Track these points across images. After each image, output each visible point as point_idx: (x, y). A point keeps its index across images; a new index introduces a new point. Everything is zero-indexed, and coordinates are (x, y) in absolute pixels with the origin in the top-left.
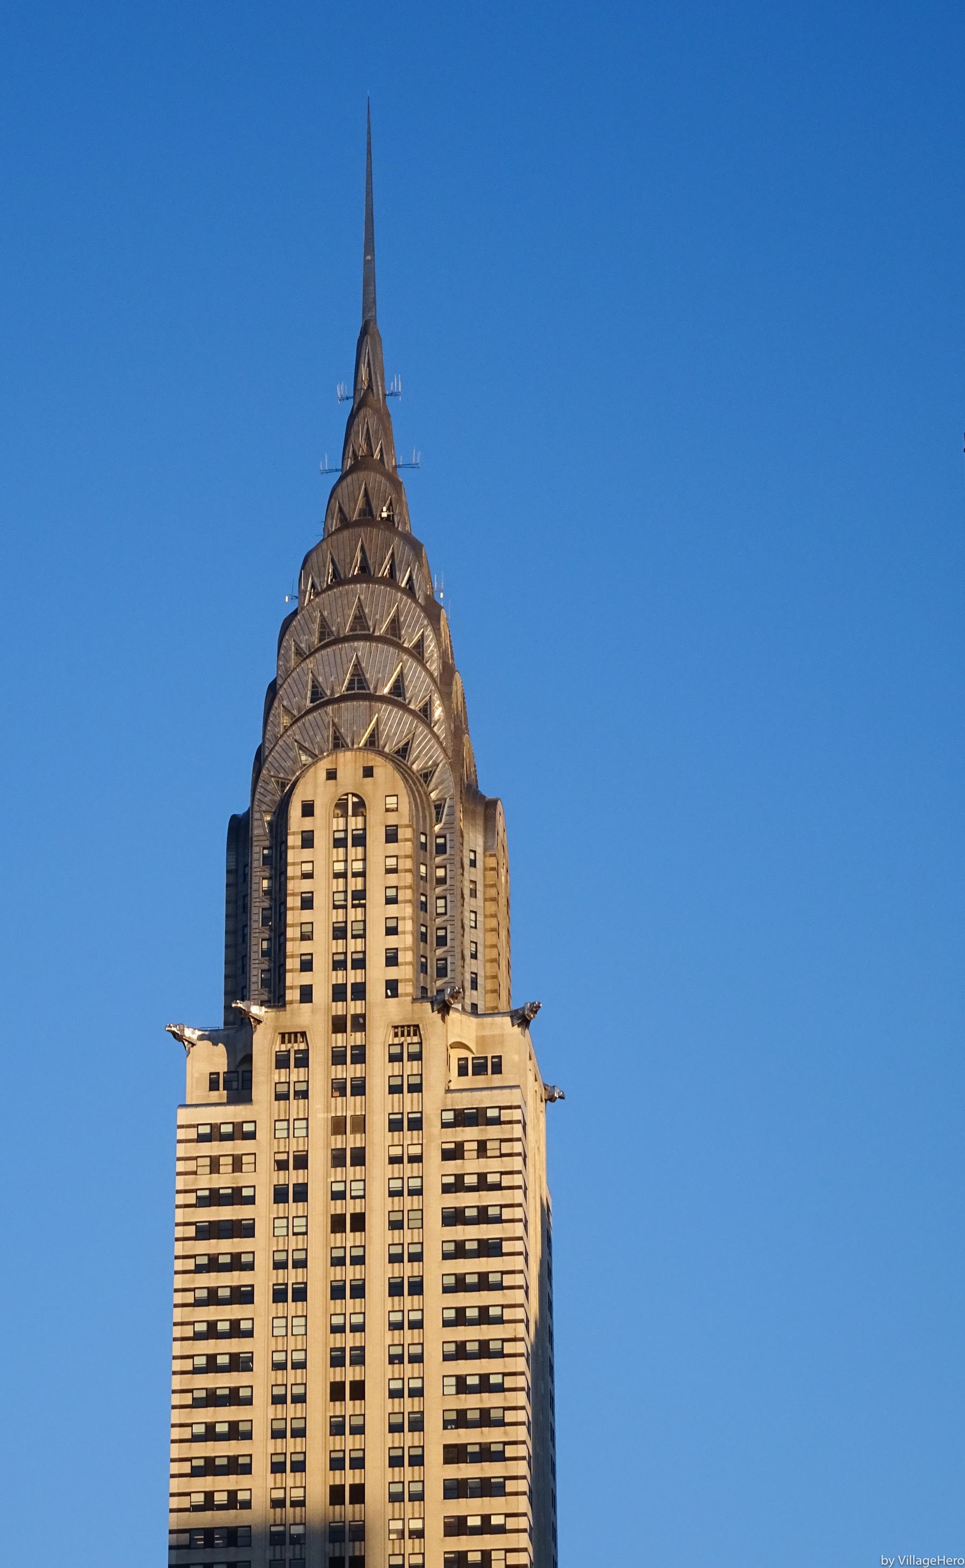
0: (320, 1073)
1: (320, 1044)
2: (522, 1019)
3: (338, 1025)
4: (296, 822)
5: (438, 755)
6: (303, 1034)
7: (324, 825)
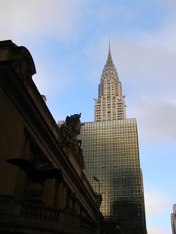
3: (108, 97)
5: (116, 77)
7: (106, 83)
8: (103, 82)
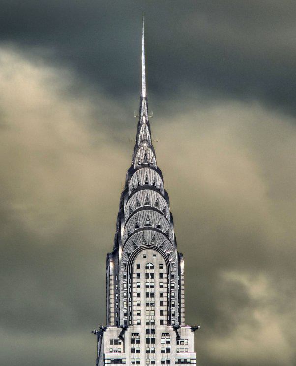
0: (142, 346)
1: (143, 337)
2: (194, 329)
3: (147, 332)
4: (136, 271)
6: (138, 334)
8: (131, 262)
